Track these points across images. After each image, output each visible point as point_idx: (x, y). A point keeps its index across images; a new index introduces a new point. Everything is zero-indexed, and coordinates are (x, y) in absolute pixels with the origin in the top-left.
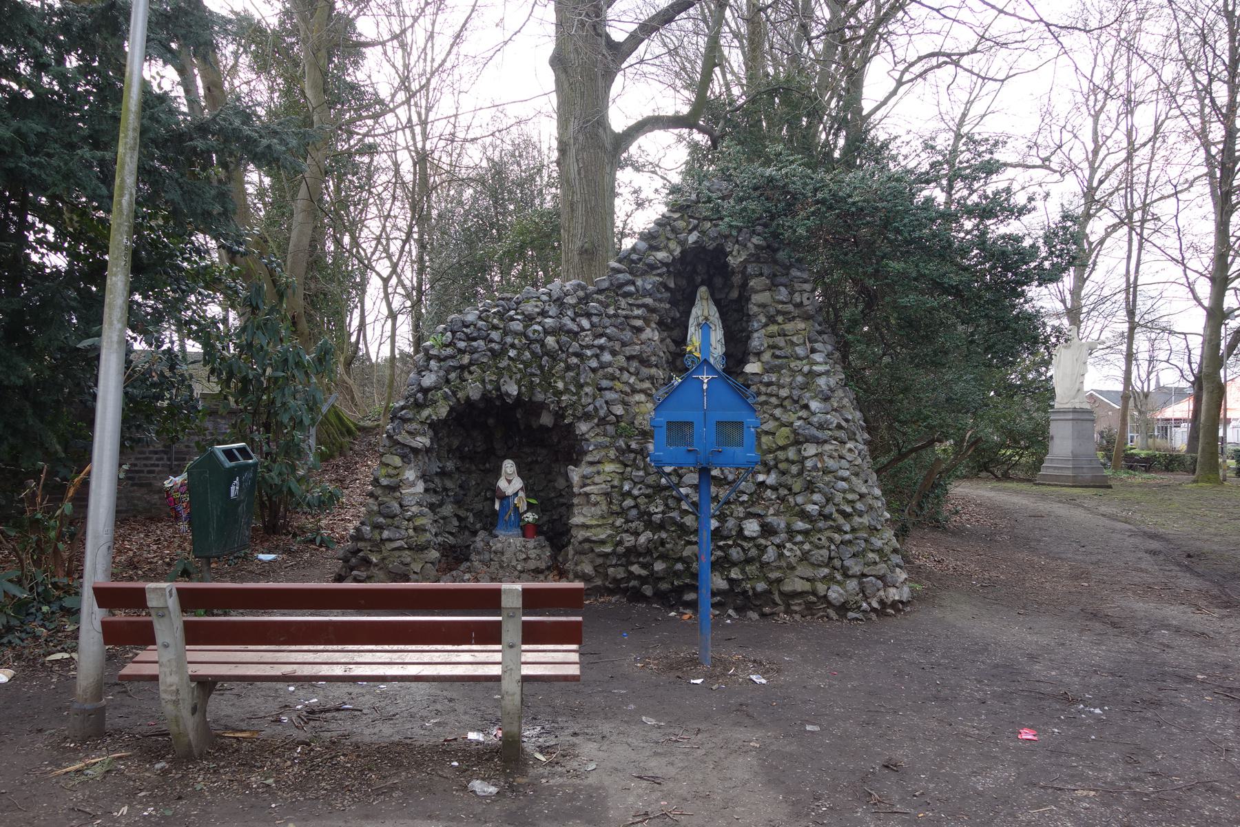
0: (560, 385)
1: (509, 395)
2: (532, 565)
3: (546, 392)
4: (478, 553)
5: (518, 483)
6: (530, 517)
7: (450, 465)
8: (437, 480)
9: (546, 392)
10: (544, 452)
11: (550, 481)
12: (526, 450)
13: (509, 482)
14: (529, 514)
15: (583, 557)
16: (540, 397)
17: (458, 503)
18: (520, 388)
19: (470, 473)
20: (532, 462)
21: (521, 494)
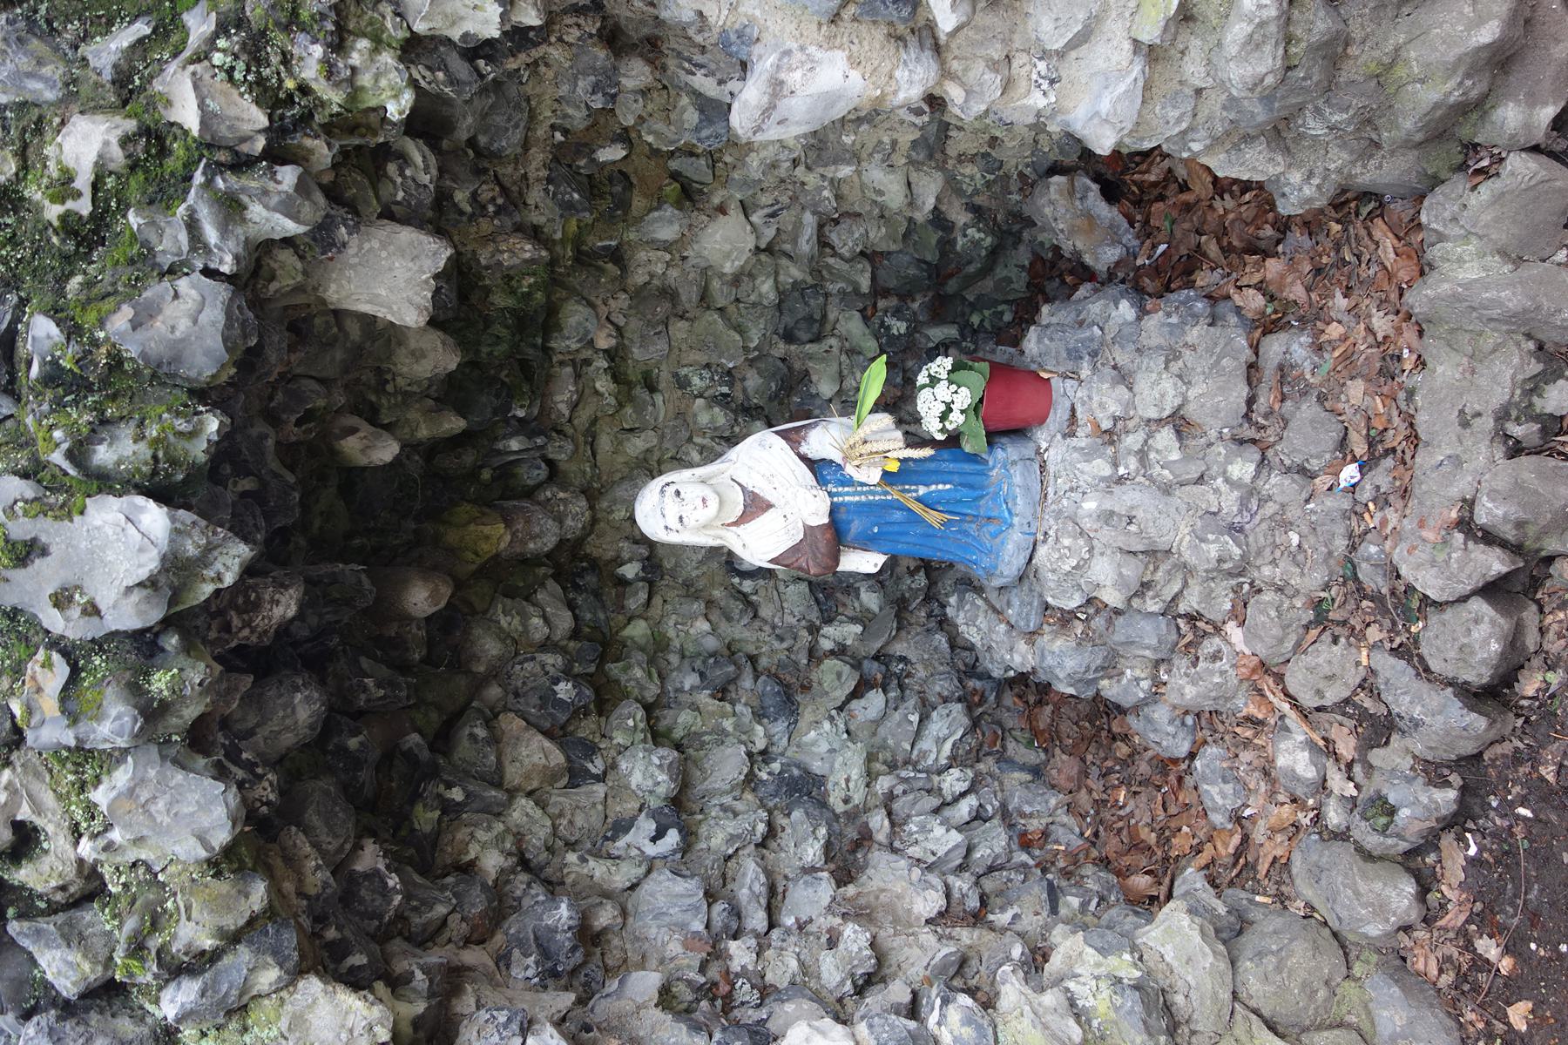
0: (86, 143)
1: (174, 573)
2: (1216, 397)
3: (146, 265)
4: (1110, 668)
5: (763, 458)
6: (944, 397)
7: (646, 773)
8: (716, 836)
9: (146, 265)
10: (575, 316)
11: (704, 298)
12: (562, 398)
13: (755, 506)
14: (929, 405)
15: (1362, 60)
16: (188, 320)
17: (788, 695)
18: (104, 482)
19: (658, 647)
20: (616, 376)
21: (824, 439)
